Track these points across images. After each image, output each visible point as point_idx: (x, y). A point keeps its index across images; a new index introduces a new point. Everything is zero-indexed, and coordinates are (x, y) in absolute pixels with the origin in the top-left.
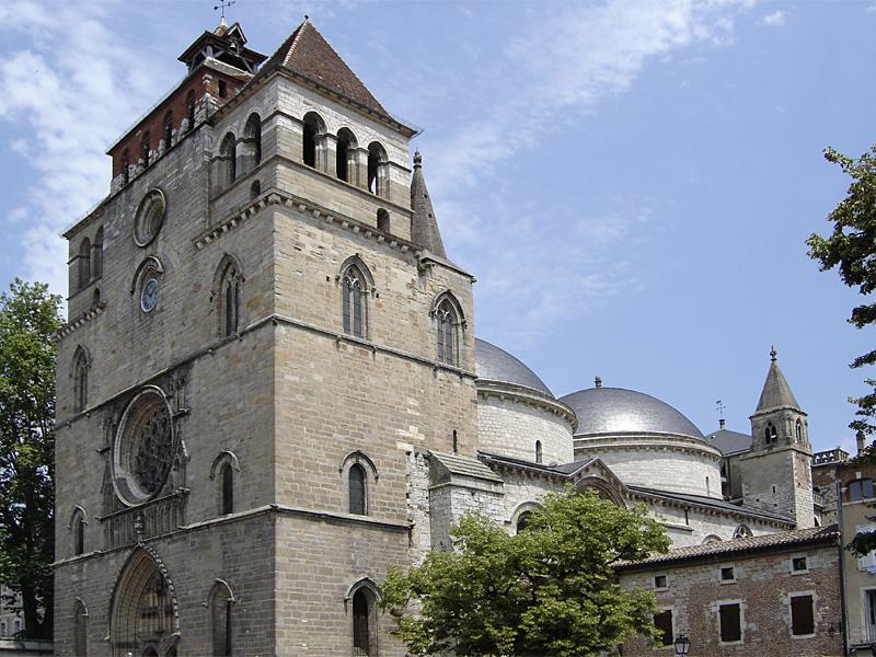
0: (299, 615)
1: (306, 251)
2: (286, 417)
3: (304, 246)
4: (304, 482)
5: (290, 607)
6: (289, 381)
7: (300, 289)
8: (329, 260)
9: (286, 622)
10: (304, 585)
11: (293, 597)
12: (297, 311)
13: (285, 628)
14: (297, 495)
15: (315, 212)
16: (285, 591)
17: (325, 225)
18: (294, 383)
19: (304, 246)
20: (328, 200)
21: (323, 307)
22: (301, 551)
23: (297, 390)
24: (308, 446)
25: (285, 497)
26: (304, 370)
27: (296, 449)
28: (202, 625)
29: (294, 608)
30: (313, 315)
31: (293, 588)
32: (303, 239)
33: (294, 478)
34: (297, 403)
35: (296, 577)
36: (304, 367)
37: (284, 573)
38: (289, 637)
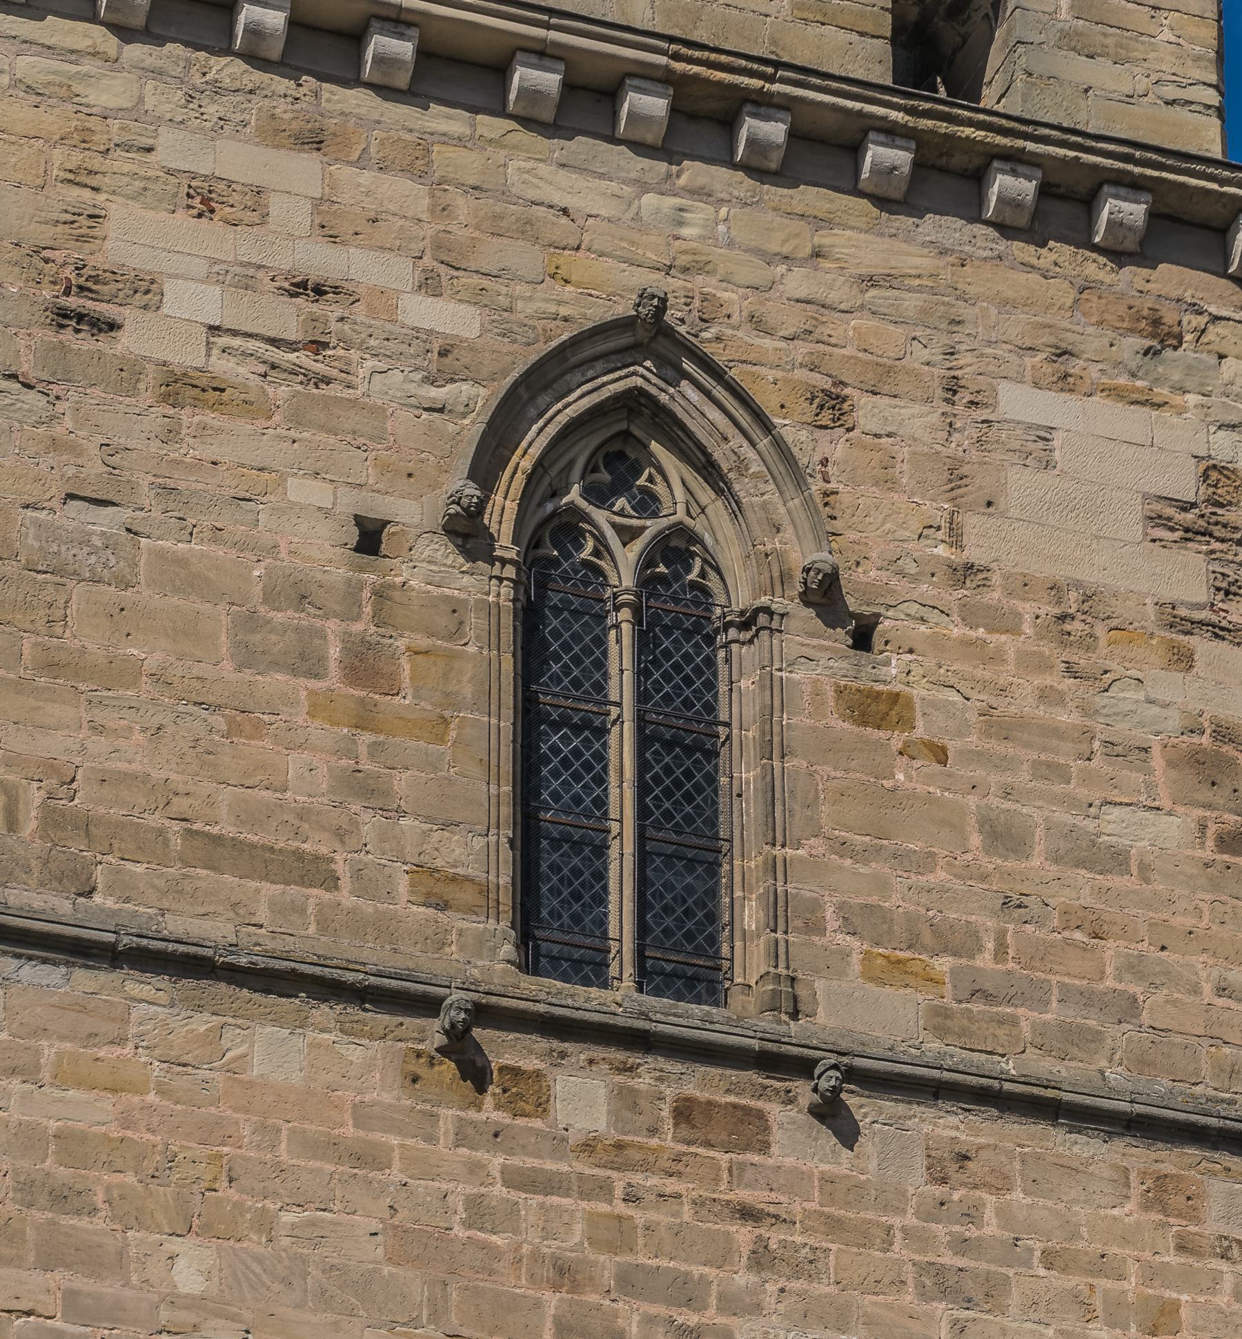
12: (52, 820)
17: (357, 101)
36: (108, 1288)
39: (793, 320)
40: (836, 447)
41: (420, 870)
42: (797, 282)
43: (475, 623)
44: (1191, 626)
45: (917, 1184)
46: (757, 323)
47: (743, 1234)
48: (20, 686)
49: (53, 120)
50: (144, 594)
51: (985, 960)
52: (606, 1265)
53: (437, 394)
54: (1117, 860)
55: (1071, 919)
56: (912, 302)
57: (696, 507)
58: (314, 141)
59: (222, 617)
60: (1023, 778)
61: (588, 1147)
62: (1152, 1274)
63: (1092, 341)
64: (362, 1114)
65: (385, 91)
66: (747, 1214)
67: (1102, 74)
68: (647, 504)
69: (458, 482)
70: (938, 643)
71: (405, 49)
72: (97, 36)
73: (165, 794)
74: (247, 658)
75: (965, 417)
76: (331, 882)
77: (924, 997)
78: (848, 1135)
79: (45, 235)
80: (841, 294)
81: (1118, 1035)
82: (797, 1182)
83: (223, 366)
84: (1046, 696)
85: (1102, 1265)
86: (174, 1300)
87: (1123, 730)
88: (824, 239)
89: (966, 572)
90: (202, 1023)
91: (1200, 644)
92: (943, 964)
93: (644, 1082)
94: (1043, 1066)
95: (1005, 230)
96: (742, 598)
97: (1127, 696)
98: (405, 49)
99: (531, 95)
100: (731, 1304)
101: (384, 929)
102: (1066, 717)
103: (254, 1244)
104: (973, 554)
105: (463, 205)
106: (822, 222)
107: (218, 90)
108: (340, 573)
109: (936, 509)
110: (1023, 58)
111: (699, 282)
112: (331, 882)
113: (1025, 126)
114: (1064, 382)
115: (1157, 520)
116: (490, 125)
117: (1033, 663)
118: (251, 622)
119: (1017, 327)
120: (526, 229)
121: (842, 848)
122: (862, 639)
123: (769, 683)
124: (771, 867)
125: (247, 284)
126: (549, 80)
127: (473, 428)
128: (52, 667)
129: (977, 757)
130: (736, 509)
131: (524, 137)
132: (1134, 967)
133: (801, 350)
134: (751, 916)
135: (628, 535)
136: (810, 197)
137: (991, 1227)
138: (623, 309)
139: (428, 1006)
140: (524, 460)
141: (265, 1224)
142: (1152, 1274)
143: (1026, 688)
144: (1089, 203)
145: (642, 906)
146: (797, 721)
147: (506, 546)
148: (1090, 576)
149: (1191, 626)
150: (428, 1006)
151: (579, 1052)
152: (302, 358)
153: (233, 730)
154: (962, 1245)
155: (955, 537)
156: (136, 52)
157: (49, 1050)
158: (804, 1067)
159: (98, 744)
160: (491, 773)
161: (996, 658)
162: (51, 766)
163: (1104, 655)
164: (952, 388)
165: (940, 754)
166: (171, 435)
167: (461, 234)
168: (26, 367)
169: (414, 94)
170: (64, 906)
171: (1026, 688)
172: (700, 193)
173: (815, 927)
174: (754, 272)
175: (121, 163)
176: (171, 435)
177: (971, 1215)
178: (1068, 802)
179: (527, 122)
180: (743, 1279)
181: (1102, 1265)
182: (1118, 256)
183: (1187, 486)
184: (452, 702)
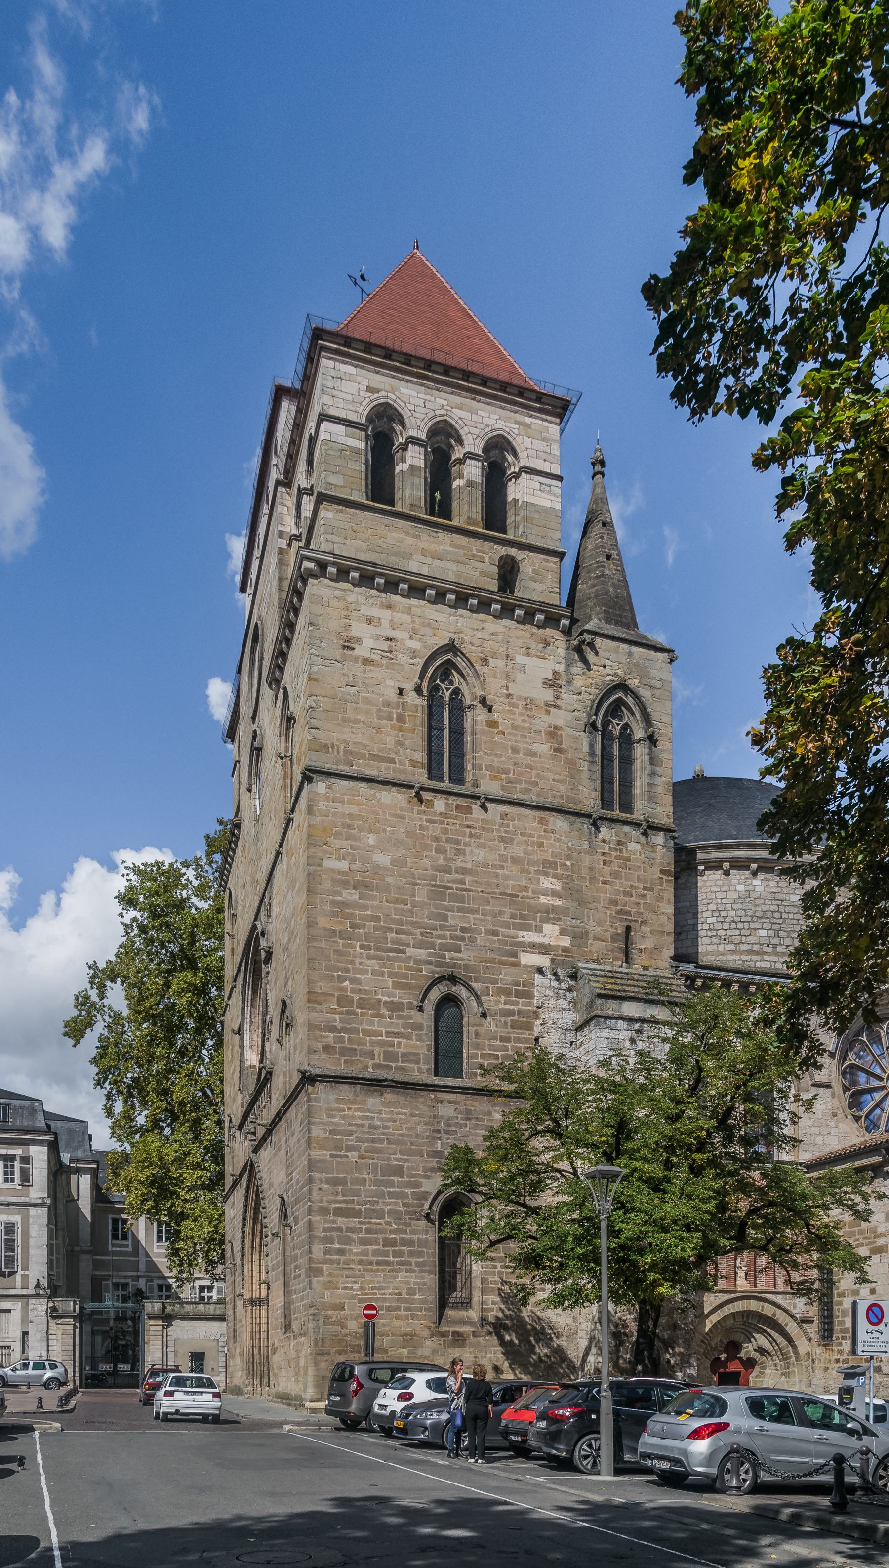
0: (349, 1241)
1: (361, 651)
2: (325, 929)
3: (359, 641)
4: (356, 1031)
5: (332, 1229)
6: (333, 871)
7: (350, 715)
8: (403, 659)
9: (327, 1252)
10: (357, 1194)
11: (339, 1212)
12: (345, 752)
13: (325, 1262)
14: (344, 1051)
15: (377, 580)
16: (325, 1204)
17: (397, 598)
18: (340, 872)
19: (359, 641)
20: (410, 556)
21: (390, 741)
22: (352, 1140)
23: (345, 884)
24: (365, 972)
25: (324, 1056)
26: (358, 849)
27: (341, 979)
28: (295, 1278)
29: (339, 1229)
30: (374, 757)
31: (340, 1198)
32: (358, 629)
33: (339, 1025)
34: (344, 904)
35: (343, 1182)
36: (357, 844)
37: (323, 1175)
38: (330, 1275)
39: (478, 643)
40: (485, 670)
41: (411, 760)
42: (479, 635)
43: (420, 709)
44: (550, 705)
45: (498, 820)
46: (471, 644)
47: (468, 831)
48: (339, 725)
49: (341, 604)
50: (360, 705)
51: (511, 775)
52: (444, 837)
53: (413, 661)
54: (534, 754)
55: (527, 766)
56: (500, 638)
57: (460, 683)
58: (389, 607)
59: (375, 709)
60: (519, 738)
61: (441, 814)
62: (540, 836)
63: (533, 645)
64: (401, 809)
65: (403, 596)
66: (468, 827)
67: (537, 586)
68: (451, 683)
69: (417, 680)
70: (504, 710)
71: (406, 586)
72: (348, 586)
73: (365, 746)
74: (380, 718)
75: (510, 663)
76: (395, 763)
77: (500, 783)
78: (486, 811)
79: (341, 630)
80: (487, 637)
81: (535, 789)
82: (477, 820)
83: (374, 657)
84: (524, 721)
85: (531, 835)
86: (369, 846)
87: (538, 728)
88: (484, 625)
89: (509, 696)
90: (373, 791)
91: (551, 709)
92: (504, 776)
93: (450, 801)
94: (521, 796)
95: (518, 622)
96: (468, 702)
97: (538, 720)
98: (406, 586)
99: (429, 595)
100: (465, 844)
101: (404, 772)
102: (527, 725)
103: (382, 834)
104: (511, 692)
105: (417, 620)
106: (484, 621)
107: (372, 597)
108: (396, 699)
109: (504, 683)
110: (523, 583)
111: (461, 635)
112: (395, 763)
113: (522, 599)
114: (528, 654)
115: (544, 683)
116: (423, 602)
117: (521, 714)
118: (379, 710)
119: (519, 643)
120: (429, 625)
121: (486, 753)
122: (490, 710)
123: (473, 720)
124: (473, 757)
125: (378, 639)
126: (433, 592)
127: (419, 668)
128: (344, 721)
129: (510, 734)
130: (467, 684)
131: (429, 605)
132: (538, 776)
133: (480, 649)
134: (469, 767)
135: (448, 689)
136: (482, 616)
137: (511, 828)
138: (447, 642)
139: (412, 787)
140: (429, 675)
141: (384, 831)
142: (540, 836)
143: (520, 719)
144: (534, 615)
145: (450, 766)
146: (478, 728)
147: (425, 693)
148: (532, 696)
149: (550, 705)
150: (412, 787)
151: (439, 796)
152: (388, 654)
153: (377, 732)
154: (506, 832)
155: (507, 689)
156: (357, 589)
157: (346, 798)
158: (478, 798)
159: (353, 736)
160: (423, 739)
161: (514, 713)
162: (345, 741)
163: (534, 713)
164: (507, 656)
165: (504, 734)
166: (364, 672)
167: (417, 626)
168: (338, 658)
169: (408, 596)
170: (348, 769)
171: (520, 719)
172: (461, 616)
173: (481, 769)
174: (471, 632)
175: (355, 613)
176: (364, 672)
177: (508, 826)
178: (527, 743)
179: (429, 602)
180: (468, 839)
181: (531, 835)
182: (539, 627)
183: (550, 677)
184: (416, 725)
